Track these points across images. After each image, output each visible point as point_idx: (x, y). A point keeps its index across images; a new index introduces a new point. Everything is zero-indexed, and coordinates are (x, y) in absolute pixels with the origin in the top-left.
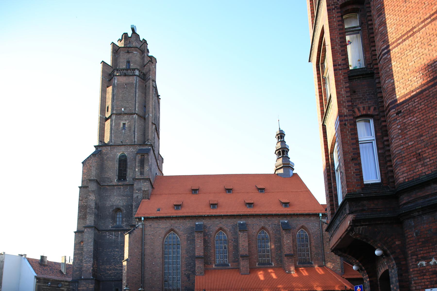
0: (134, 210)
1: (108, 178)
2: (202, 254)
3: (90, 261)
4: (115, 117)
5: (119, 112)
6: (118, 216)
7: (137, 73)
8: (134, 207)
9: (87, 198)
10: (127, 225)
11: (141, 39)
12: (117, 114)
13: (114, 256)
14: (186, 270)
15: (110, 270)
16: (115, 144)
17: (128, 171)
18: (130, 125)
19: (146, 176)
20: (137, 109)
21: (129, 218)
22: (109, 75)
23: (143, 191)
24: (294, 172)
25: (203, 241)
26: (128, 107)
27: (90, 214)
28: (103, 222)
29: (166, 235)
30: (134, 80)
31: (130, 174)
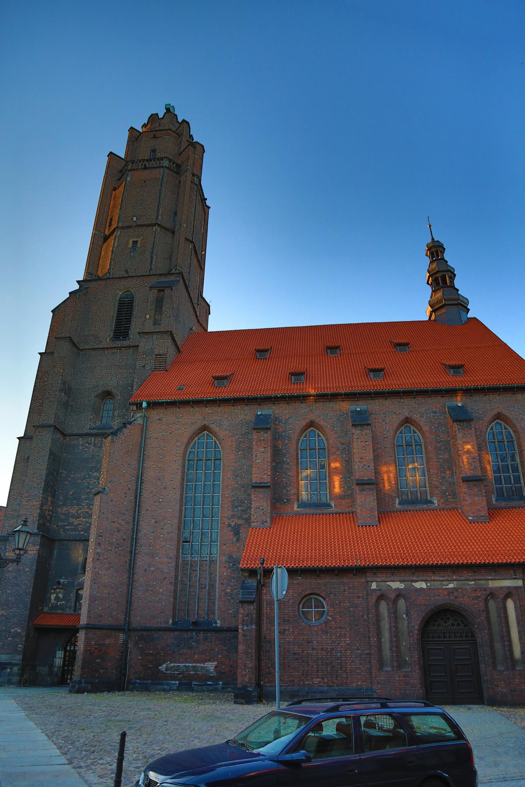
2: (267, 479)
5: (128, 224)
7: (166, 163)
11: (180, 120)
12: (123, 228)
13: (88, 488)
14: (233, 516)
15: (78, 517)
19: (162, 328)
24: (470, 315)
25: (269, 450)
29: (191, 439)
31: (135, 326)
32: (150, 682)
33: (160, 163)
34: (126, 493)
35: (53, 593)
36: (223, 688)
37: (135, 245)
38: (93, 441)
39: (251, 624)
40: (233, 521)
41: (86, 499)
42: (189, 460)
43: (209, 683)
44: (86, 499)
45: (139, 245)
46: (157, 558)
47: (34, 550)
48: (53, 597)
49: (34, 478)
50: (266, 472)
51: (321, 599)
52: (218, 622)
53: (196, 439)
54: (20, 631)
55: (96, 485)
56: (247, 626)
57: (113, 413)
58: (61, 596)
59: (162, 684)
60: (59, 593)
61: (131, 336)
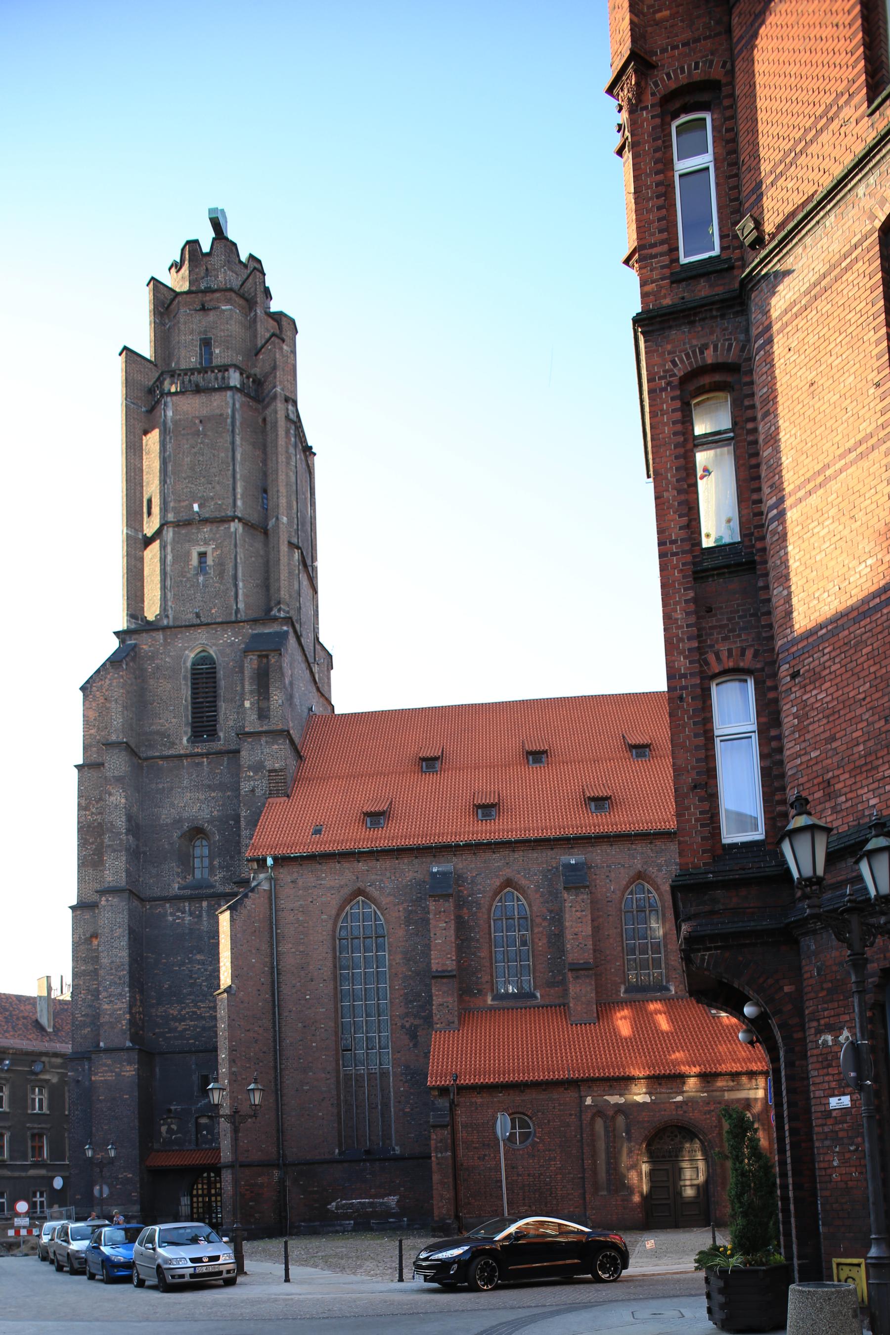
1: (163, 735)
3: (120, 994)
5: (184, 516)
6: (197, 852)
7: (235, 379)
10: (225, 880)
12: (177, 524)
13: (191, 977)
18: (220, 557)
21: (232, 857)
26: (212, 498)
27: (115, 851)
28: (154, 871)
33: (223, 378)
36: (408, 1225)
37: (203, 560)
38: (187, 908)
41: (190, 994)
44: (190, 994)
45: (210, 561)
55: (202, 973)
57: (211, 863)
61: (221, 734)
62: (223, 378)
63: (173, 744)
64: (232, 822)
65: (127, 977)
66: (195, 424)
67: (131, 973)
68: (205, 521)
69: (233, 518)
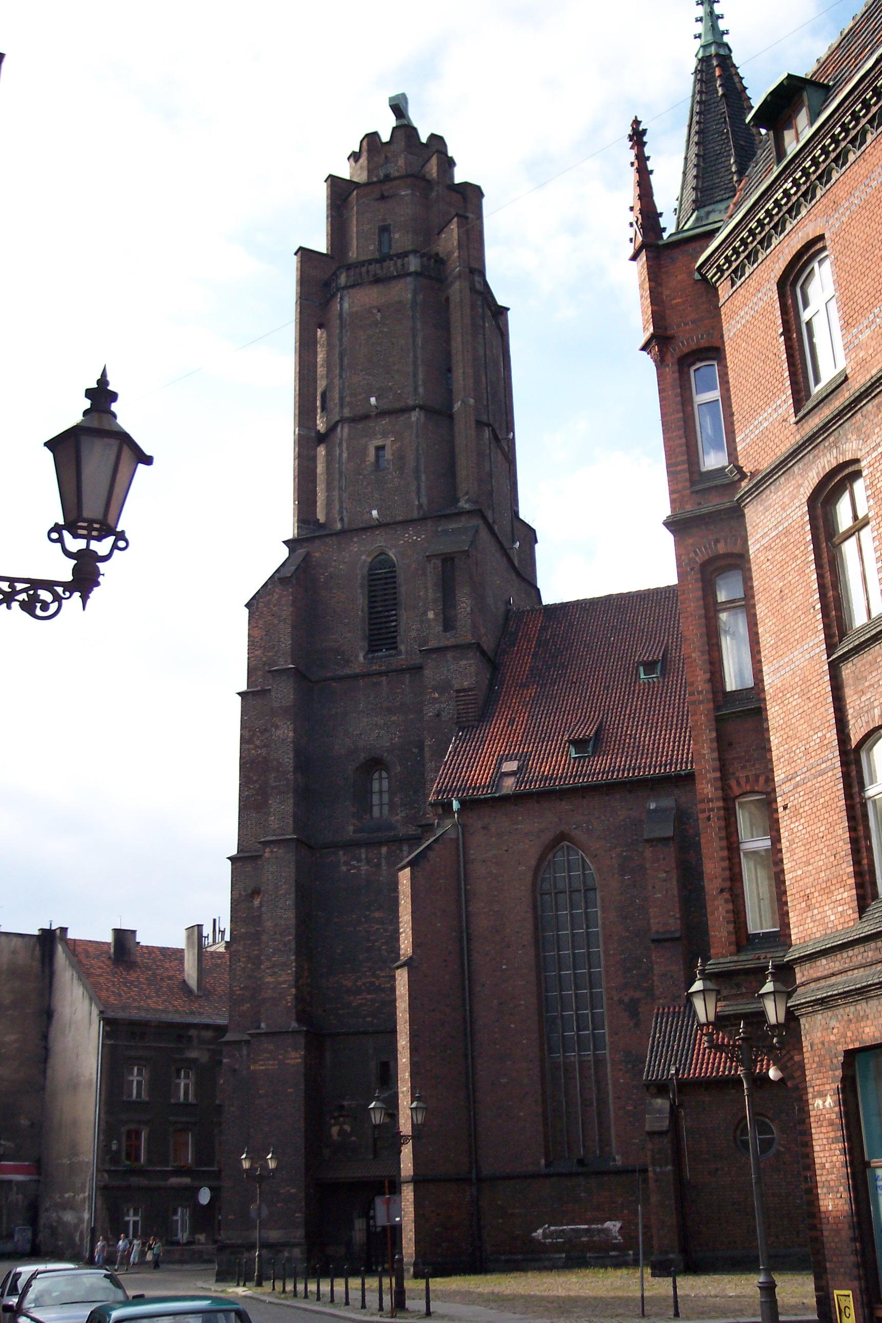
0: (430, 765)
4: (350, 427)
6: (376, 786)
8: (427, 754)
9: (266, 730)
12: (353, 420)
16: (355, 527)
17: (405, 616)
20: (421, 390)
22: (321, 281)
23: (458, 691)
30: (402, 291)
32: (520, 1257)
33: (403, 265)
34: (446, 961)
35: (335, 1125)
37: (381, 453)
38: (363, 856)
39: (666, 1165)
40: (626, 995)
42: (541, 895)
43: (613, 1253)
45: (388, 454)
46: (509, 1063)
47: (296, 1058)
48: (335, 1130)
49: (275, 933)
50: (672, 913)
51: (767, 1120)
52: (617, 1157)
53: (550, 856)
54: (293, 1191)
56: (661, 1167)
57: (391, 800)
58: (347, 1128)
59: (540, 1260)
60: (344, 1123)
61: (402, 648)
62: (403, 265)
63: (348, 661)
64: (415, 750)
65: (293, 942)
66: (372, 313)
67: (298, 937)
68: (383, 413)
69: (413, 408)
